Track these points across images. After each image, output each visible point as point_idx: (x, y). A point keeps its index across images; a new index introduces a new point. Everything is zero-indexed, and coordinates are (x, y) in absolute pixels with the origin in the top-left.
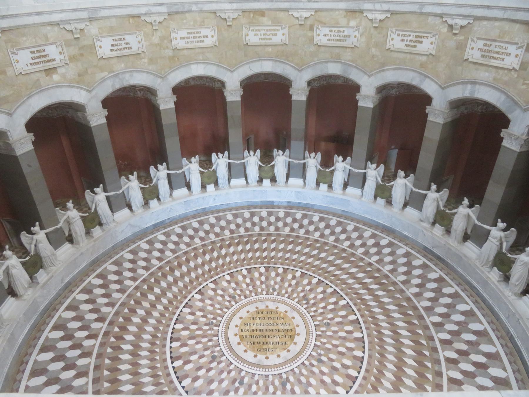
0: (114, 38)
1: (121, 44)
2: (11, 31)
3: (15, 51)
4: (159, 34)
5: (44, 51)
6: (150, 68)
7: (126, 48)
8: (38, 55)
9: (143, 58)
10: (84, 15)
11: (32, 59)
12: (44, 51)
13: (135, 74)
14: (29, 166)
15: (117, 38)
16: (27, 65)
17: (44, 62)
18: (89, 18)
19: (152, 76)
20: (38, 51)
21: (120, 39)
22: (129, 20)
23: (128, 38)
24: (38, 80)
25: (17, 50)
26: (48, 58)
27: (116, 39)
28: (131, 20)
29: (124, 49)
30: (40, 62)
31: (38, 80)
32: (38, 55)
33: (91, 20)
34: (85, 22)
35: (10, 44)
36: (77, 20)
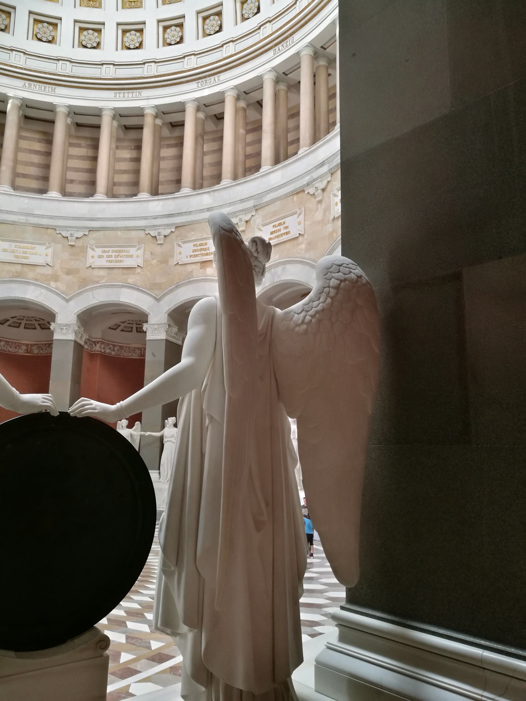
0: (274, 224)
1: (280, 230)
2: (184, 227)
3: (180, 243)
4: (323, 205)
5: (206, 244)
6: (307, 256)
7: (284, 234)
8: (199, 248)
9: (301, 244)
10: (250, 204)
11: (193, 252)
12: (206, 244)
13: (289, 267)
14: (153, 355)
15: (277, 223)
16: (187, 257)
17: (203, 255)
18: (254, 206)
19: (307, 268)
20: (201, 245)
21: (280, 224)
22: (293, 199)
23: (289, 221)
24: (192, 272)
25: (184, 242)
26: (208, 252)
27: (276, 225)
28: (295, 197)
29: (282, 235)
30: (199, 254)
31: (192, 272)
32: (199, 248)
33: (257, 208)
34: (251, 212)
35: (179, 238)
36: (243, 210)
